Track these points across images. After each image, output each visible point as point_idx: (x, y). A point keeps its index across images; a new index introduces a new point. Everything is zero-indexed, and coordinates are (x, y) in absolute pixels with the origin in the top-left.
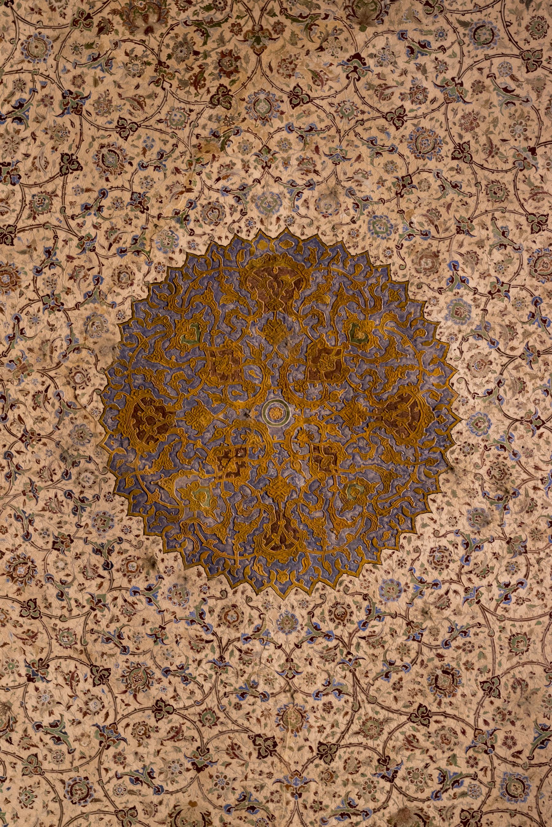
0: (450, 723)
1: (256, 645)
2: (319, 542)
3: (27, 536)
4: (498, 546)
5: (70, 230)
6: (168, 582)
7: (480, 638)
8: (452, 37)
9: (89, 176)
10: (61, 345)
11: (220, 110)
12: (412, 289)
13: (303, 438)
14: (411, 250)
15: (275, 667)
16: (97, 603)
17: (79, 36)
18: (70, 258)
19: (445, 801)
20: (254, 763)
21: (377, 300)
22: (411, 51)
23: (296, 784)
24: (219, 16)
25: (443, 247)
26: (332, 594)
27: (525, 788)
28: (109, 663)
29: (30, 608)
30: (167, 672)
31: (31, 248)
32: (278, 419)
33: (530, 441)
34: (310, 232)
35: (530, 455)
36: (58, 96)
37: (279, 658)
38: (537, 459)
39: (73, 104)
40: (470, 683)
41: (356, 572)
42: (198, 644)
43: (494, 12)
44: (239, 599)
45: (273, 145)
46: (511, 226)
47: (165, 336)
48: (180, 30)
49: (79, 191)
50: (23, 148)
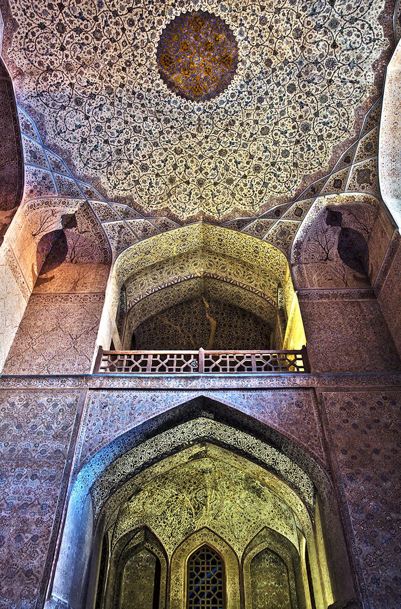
0: (232, 132)
1: (192, 114)
2: (206, 91)
3: (141, 89)
4: (246, 93)
5: (146, 9)
6: (173, 99)
7: (240, 114)
10: (146, 41)
12: (230, 26)
13: (203, 65)
14: (231, 15)
16: (157, 104)
18: (146, 17)
19: (230, 148)
20: (192, 139)
23: (200, 143)
26: (209, 103)
27: (247, 146)
29: (143, 105)
30: (173, 119)
31: (136, 14)
32: (197, 61)
34: (206, 10)
35: (255, 71)
40: (237, 123)
44: (188, 104)
46: (256, 9)
47: (170, 39)
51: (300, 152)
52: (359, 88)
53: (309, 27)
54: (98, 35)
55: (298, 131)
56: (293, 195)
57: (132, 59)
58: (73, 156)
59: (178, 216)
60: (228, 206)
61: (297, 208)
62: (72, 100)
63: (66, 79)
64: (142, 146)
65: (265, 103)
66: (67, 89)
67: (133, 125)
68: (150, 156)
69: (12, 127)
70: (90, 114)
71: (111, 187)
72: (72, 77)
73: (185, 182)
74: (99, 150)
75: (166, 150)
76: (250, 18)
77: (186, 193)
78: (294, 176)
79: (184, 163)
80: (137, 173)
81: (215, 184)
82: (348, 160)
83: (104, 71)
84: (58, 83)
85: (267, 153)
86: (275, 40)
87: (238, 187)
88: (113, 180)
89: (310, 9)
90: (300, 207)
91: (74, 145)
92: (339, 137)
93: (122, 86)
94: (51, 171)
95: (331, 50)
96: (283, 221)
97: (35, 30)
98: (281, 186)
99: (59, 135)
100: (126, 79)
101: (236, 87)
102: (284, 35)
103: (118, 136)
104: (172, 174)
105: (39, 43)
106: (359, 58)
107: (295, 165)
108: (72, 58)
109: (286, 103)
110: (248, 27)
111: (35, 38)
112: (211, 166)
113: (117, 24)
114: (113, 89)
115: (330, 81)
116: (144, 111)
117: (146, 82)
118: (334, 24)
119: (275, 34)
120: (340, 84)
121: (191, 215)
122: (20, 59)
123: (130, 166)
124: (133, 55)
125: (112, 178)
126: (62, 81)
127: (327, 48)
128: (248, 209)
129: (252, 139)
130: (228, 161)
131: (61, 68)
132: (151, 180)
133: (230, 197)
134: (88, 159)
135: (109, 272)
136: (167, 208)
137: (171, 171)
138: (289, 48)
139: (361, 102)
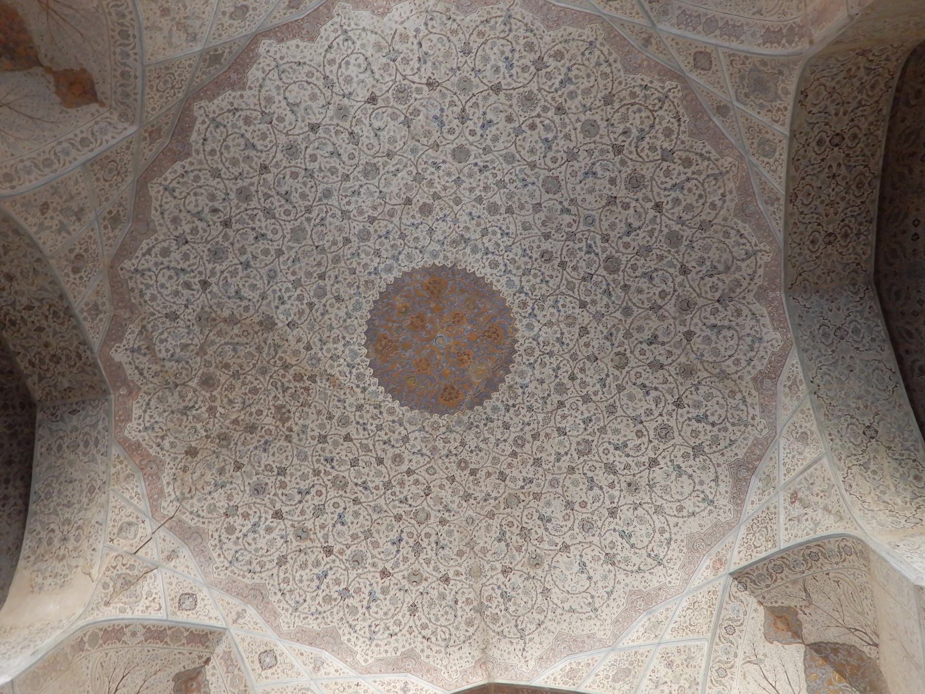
0: (564, 252)
1: (541, 339)
3: (505, 441)
4: (485, 240)
6: (518, 380)
7: (526, 243)
8: (275, 287)
9: (352, 429)
10: (423, 434)
11: (318, 379)
16: (530, 409)
17: (295, 439)
19: (599, 250)
20: (591, 335)
21: (388, 304)
22: (283, 303)
23: (598, 317)
25: (362, 279)
26: (515, 309)
29: (535, 437)
30: (556, 377)
33: (439, 232)
34: (363, 336)
35: (444, 232)
36: (320, 445)
37: (545, 329)
38: (446, 228)
39: (323, 439)
42: (544, 365)
43: (262, 271)
44: (522, 349)
45: (329, 355)
48: (287, 399)
49: (358, 433)
50: (344, 458)
51: (580, 97)
53: (356, 154)
54: (422, 516)
55: (539, 116)
56: (674, 84)
57: (453, 458)
58: (641, 587)
59: (773, 354)
60: (733, 233)
61: (696, 66)
62: (532, 574)
64: (618, 439)
65: (497, 199)
67: (576, 456)
68: (637, 420)
71: (711, 512)
73: (689, 341)
74: (631, 528)
75: (620, 388)
77: (714, 338)
78: (633, 95)
79: (645, 346)
81: (685, 271)
83: (478, 510)
85: (597, 168)
86: (388, 207)
87: (686, 217)
89: (332, 160)
90: (691, 59)
91: (619, 582)
93: (502, 476)
94: (659, 644)
95: (380, 103)
96: (732, 93)
97: (418, 623)
98: (662, 118)
99: (596, 610)
100: (490, 470)
101: (477, 261)
102: (377, 194)
105: (437, 620)
106: (378, 47)
107: (608, 100)
109: (489, 157)
111: (430, 625)
112: (644, 286)
113: (402, 484)
116: (547, 435)
119: (380, 210)
120: (429, 64)
121: (767, 321)
122: (461, 658)
125: (689, 505)
127: (380, 110)
128: (731, 185)
129: (574, 210)
131: (477, 586)
133: (710, 232)
134: (649, 556)
135: (880, 557)
136: (754, 379)
138: (395, 179)
139: (448, 10)
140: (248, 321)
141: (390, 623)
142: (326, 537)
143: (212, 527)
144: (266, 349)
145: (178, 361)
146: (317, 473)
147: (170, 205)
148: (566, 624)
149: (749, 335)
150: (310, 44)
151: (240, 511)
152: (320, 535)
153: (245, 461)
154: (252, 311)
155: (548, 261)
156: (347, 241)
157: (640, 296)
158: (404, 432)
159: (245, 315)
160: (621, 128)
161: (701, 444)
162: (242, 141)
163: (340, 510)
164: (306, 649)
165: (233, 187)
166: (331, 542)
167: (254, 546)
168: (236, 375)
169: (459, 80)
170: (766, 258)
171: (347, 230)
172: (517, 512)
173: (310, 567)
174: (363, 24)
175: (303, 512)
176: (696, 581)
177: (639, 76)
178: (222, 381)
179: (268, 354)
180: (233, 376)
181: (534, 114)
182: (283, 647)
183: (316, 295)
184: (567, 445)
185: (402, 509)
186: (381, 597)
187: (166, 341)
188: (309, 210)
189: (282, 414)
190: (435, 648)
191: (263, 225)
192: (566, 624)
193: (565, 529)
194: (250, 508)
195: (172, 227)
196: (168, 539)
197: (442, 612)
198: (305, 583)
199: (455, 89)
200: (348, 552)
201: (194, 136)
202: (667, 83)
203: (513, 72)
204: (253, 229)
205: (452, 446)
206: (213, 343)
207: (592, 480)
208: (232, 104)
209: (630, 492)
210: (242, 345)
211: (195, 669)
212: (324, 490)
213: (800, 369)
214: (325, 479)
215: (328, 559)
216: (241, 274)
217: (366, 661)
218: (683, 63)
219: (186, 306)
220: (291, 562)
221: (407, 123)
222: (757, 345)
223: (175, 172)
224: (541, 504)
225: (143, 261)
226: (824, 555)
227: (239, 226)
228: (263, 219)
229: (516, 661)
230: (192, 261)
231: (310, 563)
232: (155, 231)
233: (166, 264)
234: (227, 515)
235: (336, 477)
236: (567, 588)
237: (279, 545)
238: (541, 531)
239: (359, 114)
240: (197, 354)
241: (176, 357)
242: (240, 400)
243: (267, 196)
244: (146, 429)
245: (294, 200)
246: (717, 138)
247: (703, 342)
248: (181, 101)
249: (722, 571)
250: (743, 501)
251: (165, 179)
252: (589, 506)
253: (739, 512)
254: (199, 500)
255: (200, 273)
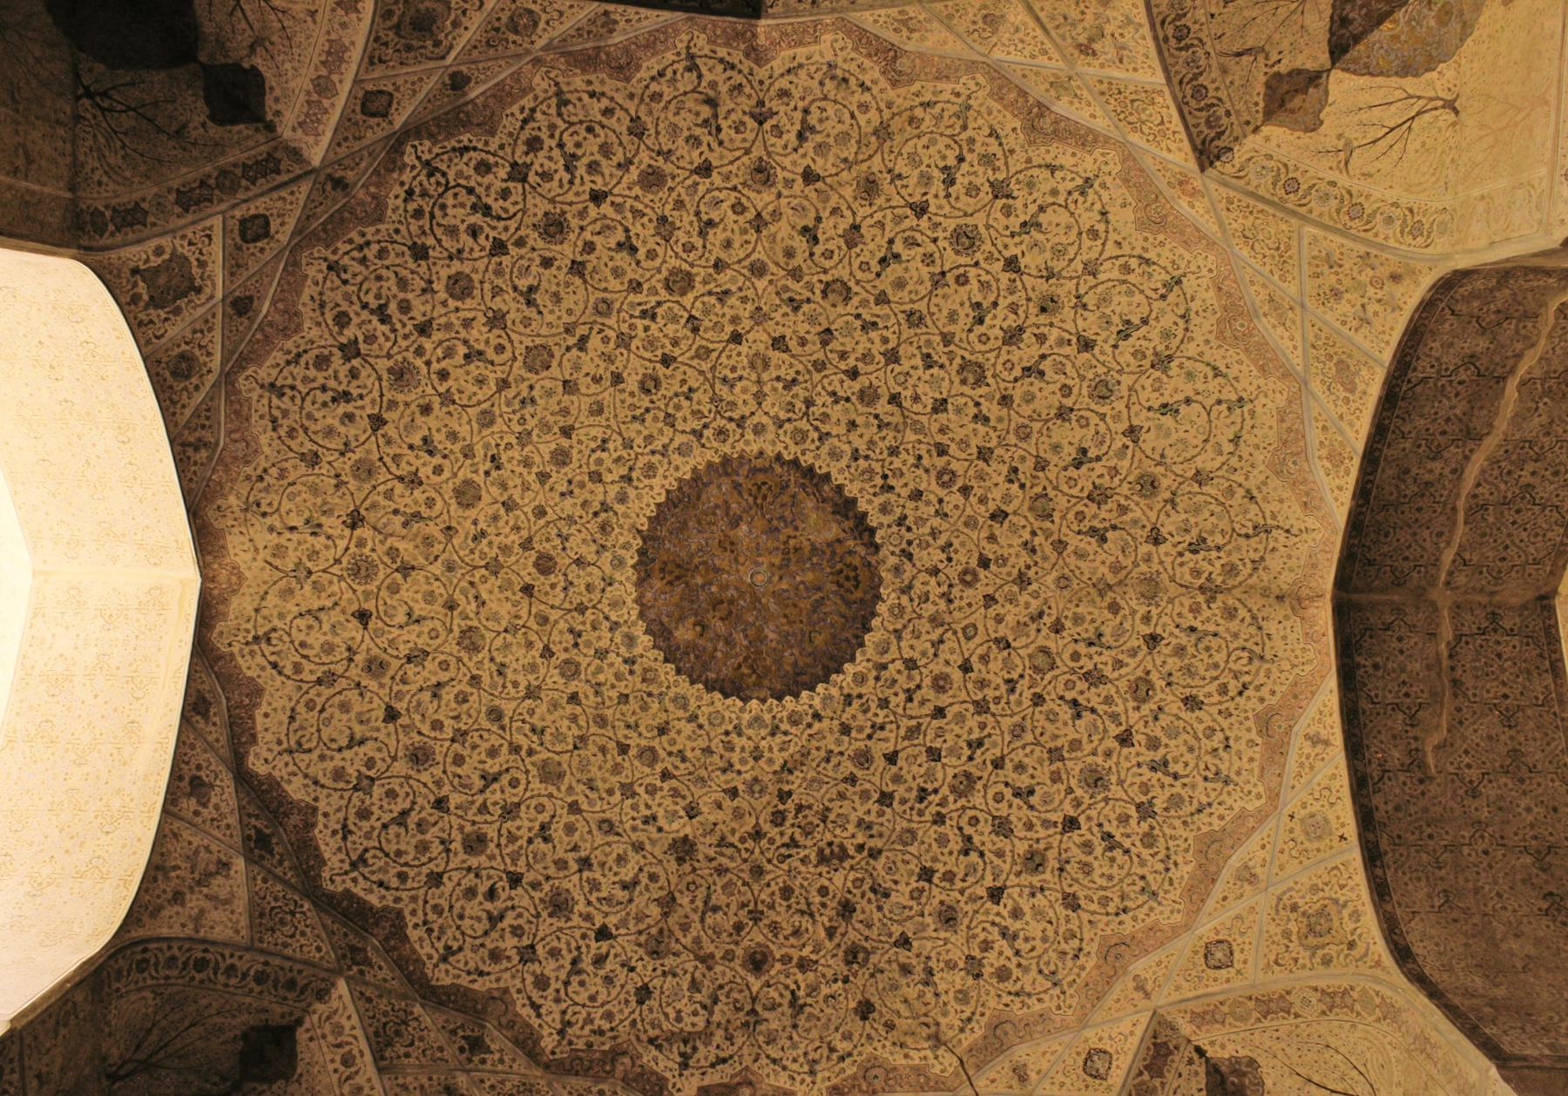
0: (647, 355)
1: (783, 415)
2: (737, 486)
3: (941, 501)
4: (608, 478)
7: (624, 414)
9: (879, 749)
10: (906, 635)
11: (786, 788)
15: (769, 400)
16: (894, 451)
19: (653, 300)
20: (788, 333)
22: (654, 818)
23: (759, 317)
24: (783, 851)
26: (727, 449)
28: (889, 408)
29: (942, 451)
30: (848, 400)
31: (923, 703)
33: (584, 550)
34: (729, 701)
37: (766, 405)
39: (886, 799)
40: (632, 383)
41: (710, 465)
42: (825, 417)
44: (793, 448)
45: (751, 762)
48: (809, 843)
49: (886, 740)
51: (410, 296)
52: (264, 514)
54: (1041, 660)
55: (428, 363)
56: (409, 149)
57: (955, 592)
58: (1213, 319)
59: (855, 49)
60: (654, 87)
62: (1167, 495)
63: (1168, 560)
64: (966, 316)
65: (546, 450)
66: (1172, 529)
67: (983, 390)
68: (938, 280)
69: (1386, 473)
70: (1120, 441)
71: (1104, 186)
72: (1148, 560)
73: (818, 178)
74: (1116, 319)
75: (882, 299)
76: (606, 676)
77: (819, 138)
78: (418, 214)
79: (818, 250)
80: (991, 221)
81: (705, 170)
82: (241, 306)
83: (1047, 566)
84: (1195, 552)
85: (523, 284)
86: (532, 623)
87: (619, 157)
88: (1089, 210)
91: (1201, 354)
92: (288, 363)
93: (999, 516)
95: (369, 606)
98: (460, 174)
99: (1241, 399)
100: (984, 534)
101: (639, 497)
103: (1043, 357)
104: (869, 211)
105: (1216, 666)
106: (290, 591)
107: (420, 253)
108: (1134, 612)
109: (479, 450)
110: (612, 656)
111: (1222, 680)
113: (982, 684)
114: (1031, 509)
115: (355, 520)
116: (942, 431)
117: (921, 521)
118: (375, 667)
119: (534, 637)
120: (323, 520)
121: (801, 52)
122: (1284, 638)
123: (1017, 251)
124: (950, 601)
125: (1089, 219)
126: (1181, 554)
128: (578, 82)
129: (582, 330)
130: (660, 251)
131: (1173, 590)
132: (948, 196)
133: (648, 121)
134: (1163, 297)
137: (870, 221)
139: (248, 478)
140: (674, 879)
141: (1207, 744)
142: (1046, 824)
143: (992, 1003)
144: (723, 860)
145: (715, 1001)
146: (939, 819)
147: (470, 958)
148: (1256, 453)
149: (821, 83)
150: (266, 697)
151: (976, 953)
152: (1042, 833)
153: (897, 930)
154: (658, 870)
155: (657, 384)
156: (574, 698)
157: (736, 245)
158: (899, 665)
159: (662, 881)
160: (466, 240)
161: (992, 185)
162: (393, 829)
163: (1008, 793)
164: (1218, 890)
165: (460, 858)
166: (1057, 817)
167: (1038, 943)
168: (756, 916)
169: (356, 477)
170: (701, 41)
171: (556, 695)
172: (1061, 502)
173: (1090, 859)
174: (250, 611)
175: (1000, 854)
176: (1211, 227)
177: (391, 202)
178: (760, 938)
179: (731, 858)
180: (756, 920)
181: (424, 370)
182: (1206, 929)
183: (651, 765)
184: (962, 400)
185: (1025, 691)
186: (1162, 751)
187: (679, 1012)
188: (515, 749)
189: (832, 856)
190: (1261, 679)
191: (527, 824)
192: (1256, 453)
193: (1102, 428)
194: (974, 936)
195: (505, 964)
196: (993, 1075)
197: (1205, 655)
198: (1115, 871)
199: (367, 487)
200: (1079, 792)
201: (373, 899)
202: (406, 159)
203: (355, 392)
204: (530, 841)
205: (935, 591)
206: (697, 941)
207: (1026, 370)
208: (334, 833)
209: (1055, 311)
210: (708, 897)
211: (1208, 1074)
212: (971, 813)
213: (883, 12)
214: (952, 806)
215: (1084, 827)
216: (597, 875)
217: (1259, 796)
218: (376, 132)
219: (632, 969)
220: (1076, 887)
221: (406, 569)
222: (839, 73)
223: (421, 940)
224: (1054, 459)
225: (549, 1019)
226: (1179, 17)
227: (522, 862)
228: (518, 823)
229: (1304, 548)
230: (563, 946)
231: (1084, 858)
232: (506, 991)
233: (559, 985)
234: (978, 976)
235: (953, 789)
236: (1198, 442)
237: (1045, 902)
238: (1099, 468)
239: (382, 642)
240: (710, 968)
241: (708, 1002)
242: (797, 917)
243: (483, 809)
244: (812, 1073)
245: (496, 769)
246: (502, 95)
247: (824, 155)
248: (315, 904)
249: (1198, 183)
250: (1090, 131)
251: (430, 957)
252: (1070, 382)
253: (1107, 140)
254: (945, 1014)
255: (584, 936)
